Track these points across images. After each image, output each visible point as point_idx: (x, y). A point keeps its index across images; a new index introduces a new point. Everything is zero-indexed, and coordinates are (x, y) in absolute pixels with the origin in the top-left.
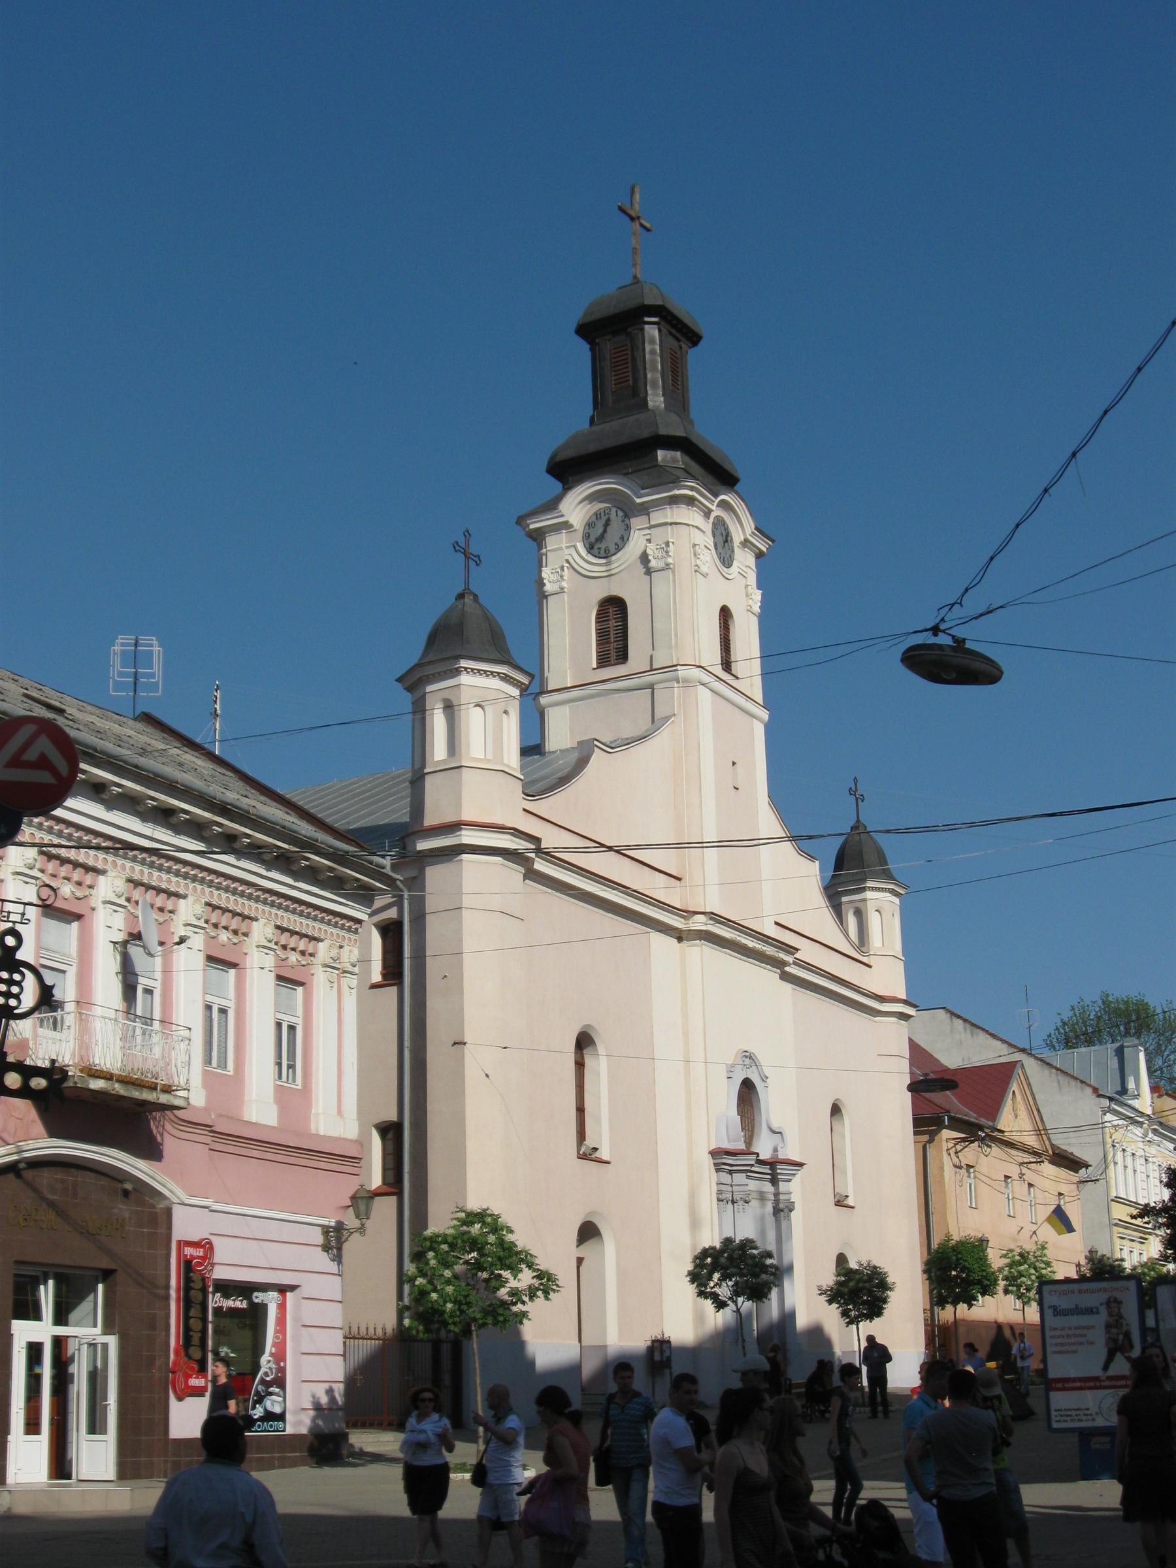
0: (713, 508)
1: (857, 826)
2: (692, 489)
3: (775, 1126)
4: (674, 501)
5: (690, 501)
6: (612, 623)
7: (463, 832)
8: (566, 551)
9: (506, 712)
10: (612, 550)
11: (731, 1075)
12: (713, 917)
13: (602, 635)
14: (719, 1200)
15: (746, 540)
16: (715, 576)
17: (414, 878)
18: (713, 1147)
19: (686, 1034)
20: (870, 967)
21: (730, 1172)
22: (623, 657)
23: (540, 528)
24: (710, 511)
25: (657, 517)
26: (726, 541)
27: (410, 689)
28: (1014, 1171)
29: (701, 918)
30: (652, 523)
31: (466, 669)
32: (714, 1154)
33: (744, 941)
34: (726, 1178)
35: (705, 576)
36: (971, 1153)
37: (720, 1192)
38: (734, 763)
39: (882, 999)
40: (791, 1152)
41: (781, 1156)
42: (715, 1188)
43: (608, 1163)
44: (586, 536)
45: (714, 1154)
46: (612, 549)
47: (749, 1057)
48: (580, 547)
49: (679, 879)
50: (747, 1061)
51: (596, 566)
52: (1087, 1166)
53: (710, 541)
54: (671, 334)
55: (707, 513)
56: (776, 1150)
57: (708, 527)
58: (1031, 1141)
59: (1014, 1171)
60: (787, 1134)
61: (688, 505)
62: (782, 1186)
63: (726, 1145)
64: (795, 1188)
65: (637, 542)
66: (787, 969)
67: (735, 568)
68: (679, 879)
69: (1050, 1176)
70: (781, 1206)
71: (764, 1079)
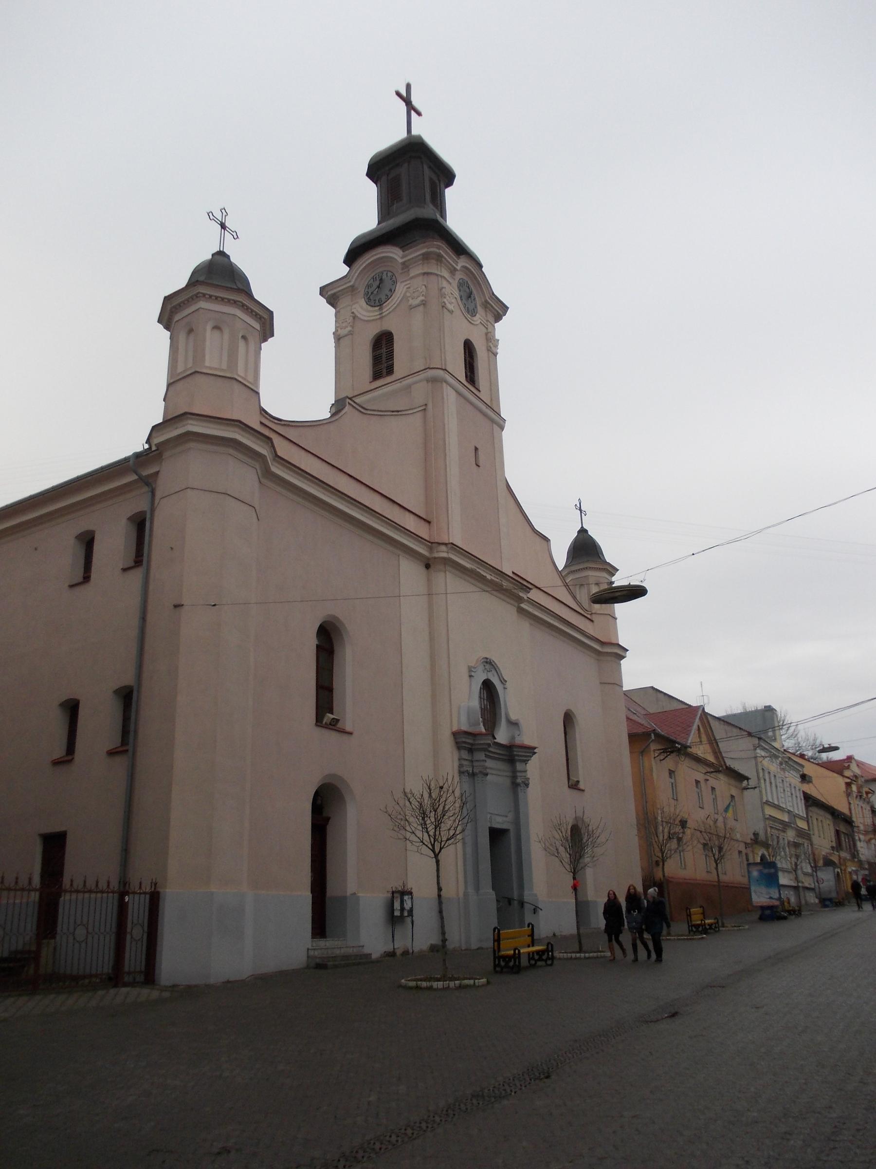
0: (458, 268)
1: (583, 531)
2: (439, 247)
3: (513, 717)
4: (426, 257)
5: (439, 258)
6: (384, 350)
7: (190, 422)
8: (354, 306)
9: (244, 337)
10: (383, 300)
11: (473, 674)
12: (453, 547)
13: (377, 360)
14: (461, 773)
15: (486, 301)
16: (457, 312)
17: (157, 473)
18: (455, 729)
19: (432, 638)
20: (592, 621)
21: (471, 751)
22: (390, 371)
23: (334, 294)
24: (455, 270)
25: (414, 272)
26: (470, 297)
27: (167, 327)
28: (701, 777)
29: (443, 548)
30: (412, 275)
31: (204, 295)
32: (455, 734)
33: (485, 574)
34: (465, 754)
35: (451, 312)
36: (670, 762)
37: (461, 766)
38: (476, 449)
39: (603, 643)
40: (527, 739)
41: (518, 741)
42: (456, 764)
43: (351, 733)
44: (366, 294)
45: (455, 734)
46: (383, 298)
47: (488, 663)
48: (362, 302)
49: (429, 522)
50: (488, 666)
51: (374, 313)
52: (747, 779)
53: (457, 294)
54: (430, 167)
55: (453, 271)
56: (513, 738)
57: (455, 284)
58: (711, 758)
59: (701, 777)
60: (522, 723)
61: (437, 260)
62: (519, 766)
63: (465, 728)
64: (532, 768)
65: (400, 289)
66: (522, 605)
67: (477, 319)
68: (429, 522)
69: (721, 783)
70: (519, 780)
71: (503, 682)
